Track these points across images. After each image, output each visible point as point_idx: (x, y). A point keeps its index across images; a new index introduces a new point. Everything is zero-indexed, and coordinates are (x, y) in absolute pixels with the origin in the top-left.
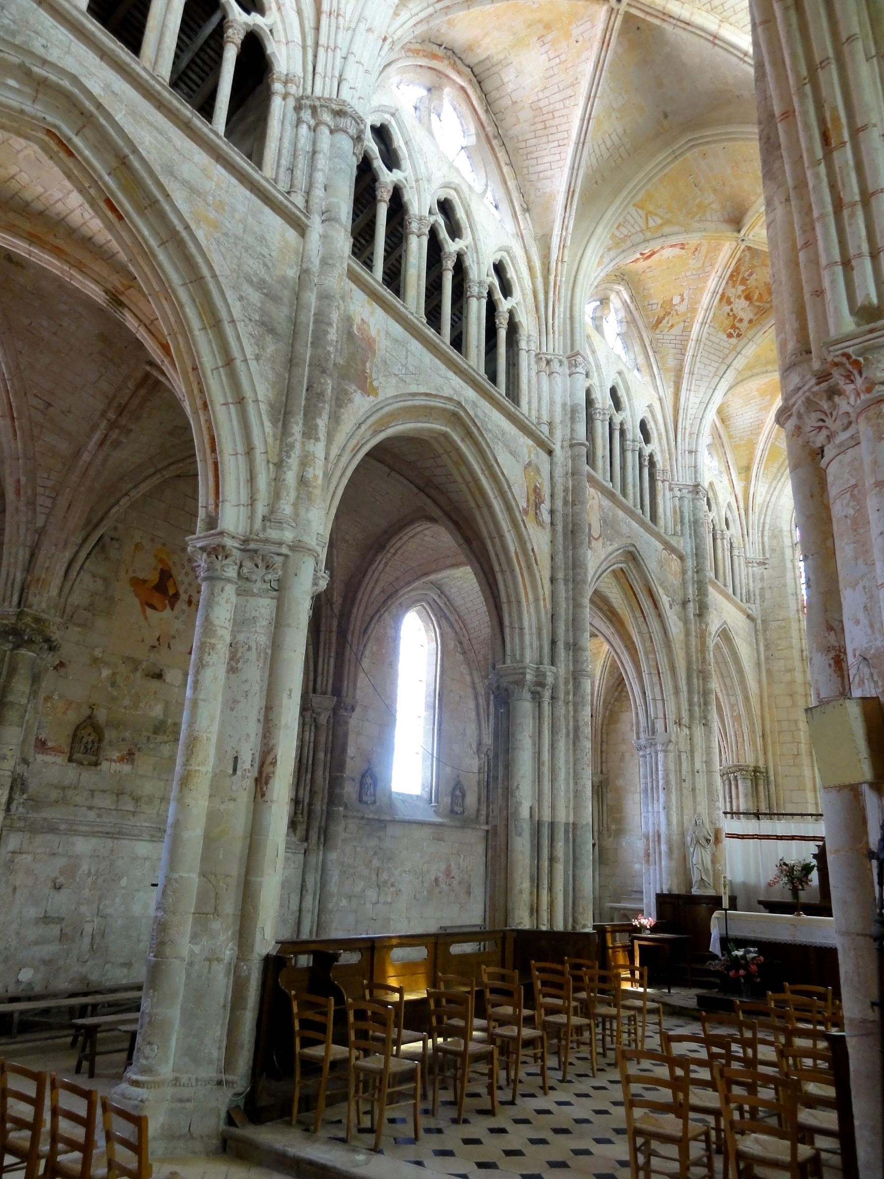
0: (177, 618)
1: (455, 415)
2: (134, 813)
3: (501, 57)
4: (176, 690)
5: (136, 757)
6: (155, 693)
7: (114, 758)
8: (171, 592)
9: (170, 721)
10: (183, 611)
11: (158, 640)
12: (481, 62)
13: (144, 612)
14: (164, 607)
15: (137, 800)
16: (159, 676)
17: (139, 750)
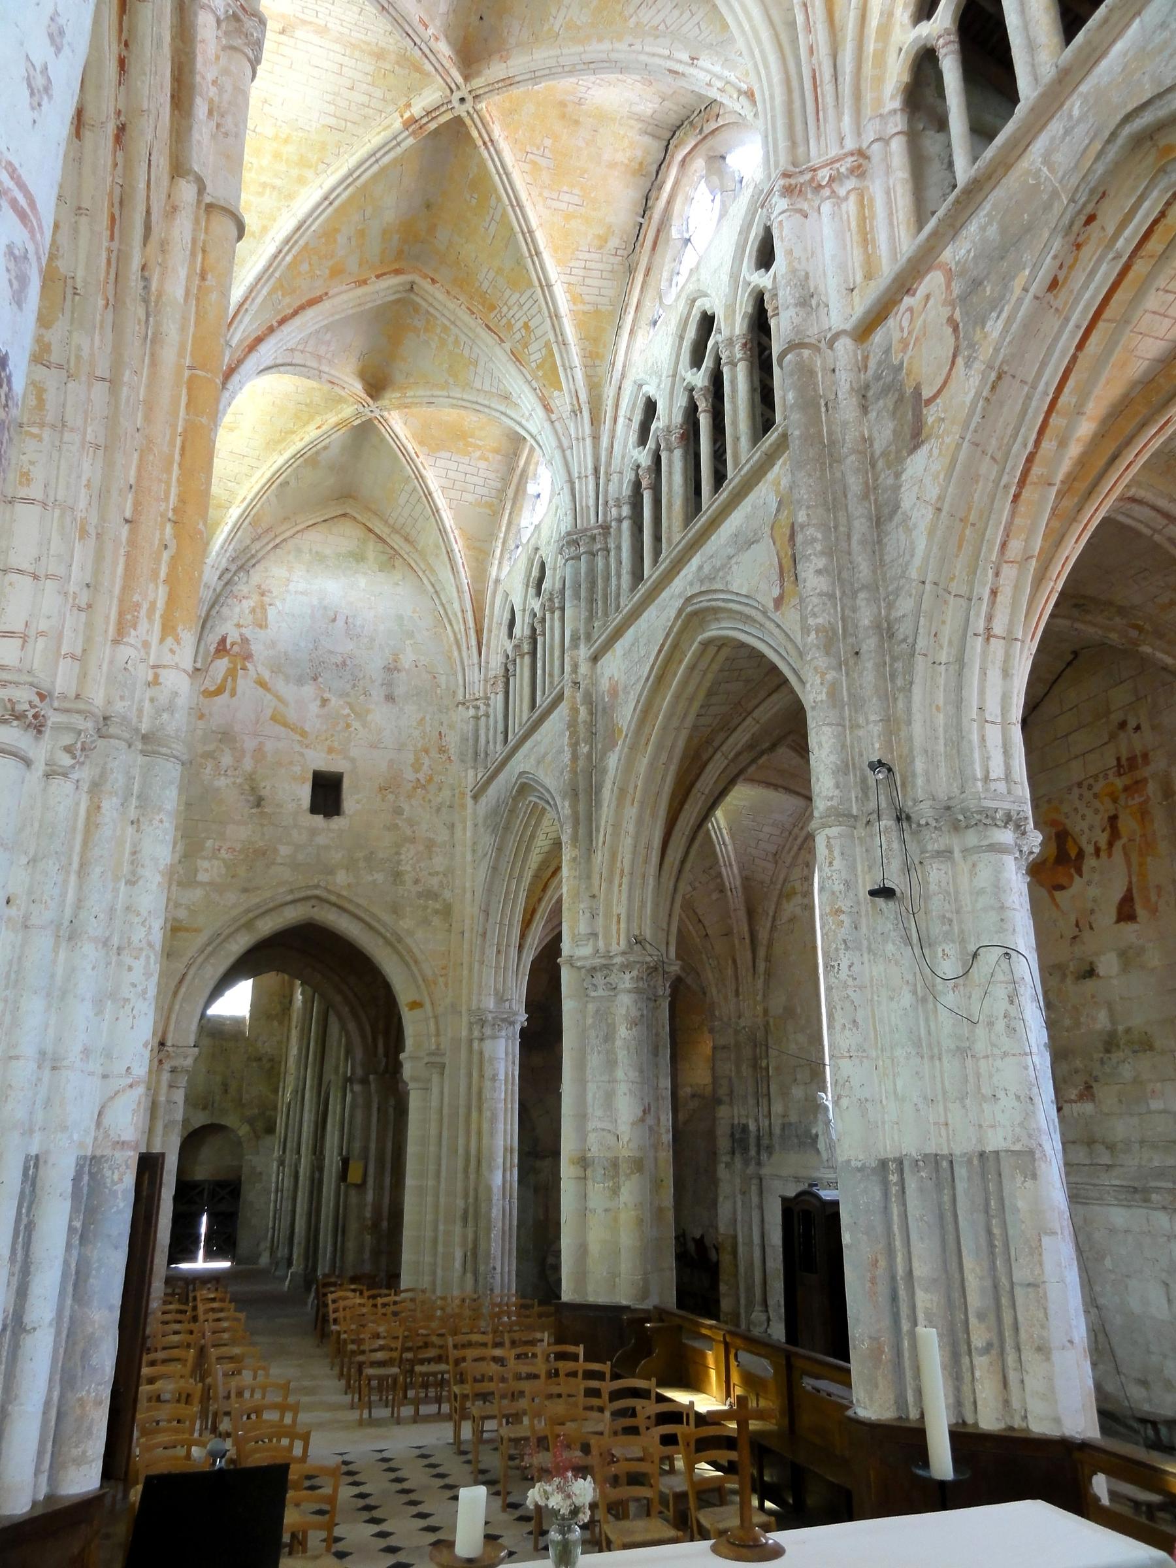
0: (1089, 883)
1: (695, 613)
2: (1109, 1167)
3: (632, 122)
4: (1115, 982)
5: (1095, 1090)
6: (1093, 996)
7: (1073, 1097)
8: (1073, 854)
9: (1120, 1028)
10: (1093, 869)
11: (1077, 925)
12: (654, 136)
13: (1053, 899)
14: (1071, 878)
15: (1111, 1147)
16: (1090, 973)
17: (1096, 1080)
